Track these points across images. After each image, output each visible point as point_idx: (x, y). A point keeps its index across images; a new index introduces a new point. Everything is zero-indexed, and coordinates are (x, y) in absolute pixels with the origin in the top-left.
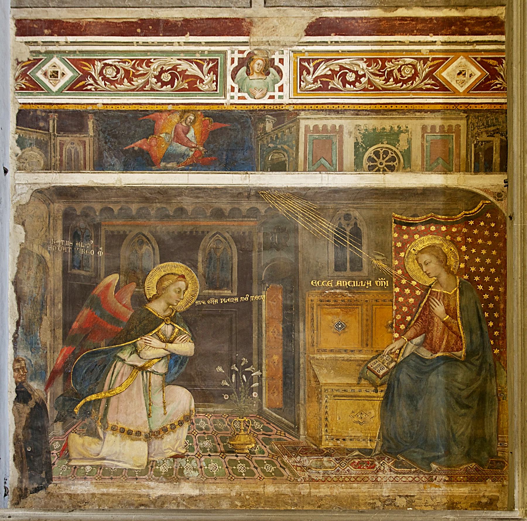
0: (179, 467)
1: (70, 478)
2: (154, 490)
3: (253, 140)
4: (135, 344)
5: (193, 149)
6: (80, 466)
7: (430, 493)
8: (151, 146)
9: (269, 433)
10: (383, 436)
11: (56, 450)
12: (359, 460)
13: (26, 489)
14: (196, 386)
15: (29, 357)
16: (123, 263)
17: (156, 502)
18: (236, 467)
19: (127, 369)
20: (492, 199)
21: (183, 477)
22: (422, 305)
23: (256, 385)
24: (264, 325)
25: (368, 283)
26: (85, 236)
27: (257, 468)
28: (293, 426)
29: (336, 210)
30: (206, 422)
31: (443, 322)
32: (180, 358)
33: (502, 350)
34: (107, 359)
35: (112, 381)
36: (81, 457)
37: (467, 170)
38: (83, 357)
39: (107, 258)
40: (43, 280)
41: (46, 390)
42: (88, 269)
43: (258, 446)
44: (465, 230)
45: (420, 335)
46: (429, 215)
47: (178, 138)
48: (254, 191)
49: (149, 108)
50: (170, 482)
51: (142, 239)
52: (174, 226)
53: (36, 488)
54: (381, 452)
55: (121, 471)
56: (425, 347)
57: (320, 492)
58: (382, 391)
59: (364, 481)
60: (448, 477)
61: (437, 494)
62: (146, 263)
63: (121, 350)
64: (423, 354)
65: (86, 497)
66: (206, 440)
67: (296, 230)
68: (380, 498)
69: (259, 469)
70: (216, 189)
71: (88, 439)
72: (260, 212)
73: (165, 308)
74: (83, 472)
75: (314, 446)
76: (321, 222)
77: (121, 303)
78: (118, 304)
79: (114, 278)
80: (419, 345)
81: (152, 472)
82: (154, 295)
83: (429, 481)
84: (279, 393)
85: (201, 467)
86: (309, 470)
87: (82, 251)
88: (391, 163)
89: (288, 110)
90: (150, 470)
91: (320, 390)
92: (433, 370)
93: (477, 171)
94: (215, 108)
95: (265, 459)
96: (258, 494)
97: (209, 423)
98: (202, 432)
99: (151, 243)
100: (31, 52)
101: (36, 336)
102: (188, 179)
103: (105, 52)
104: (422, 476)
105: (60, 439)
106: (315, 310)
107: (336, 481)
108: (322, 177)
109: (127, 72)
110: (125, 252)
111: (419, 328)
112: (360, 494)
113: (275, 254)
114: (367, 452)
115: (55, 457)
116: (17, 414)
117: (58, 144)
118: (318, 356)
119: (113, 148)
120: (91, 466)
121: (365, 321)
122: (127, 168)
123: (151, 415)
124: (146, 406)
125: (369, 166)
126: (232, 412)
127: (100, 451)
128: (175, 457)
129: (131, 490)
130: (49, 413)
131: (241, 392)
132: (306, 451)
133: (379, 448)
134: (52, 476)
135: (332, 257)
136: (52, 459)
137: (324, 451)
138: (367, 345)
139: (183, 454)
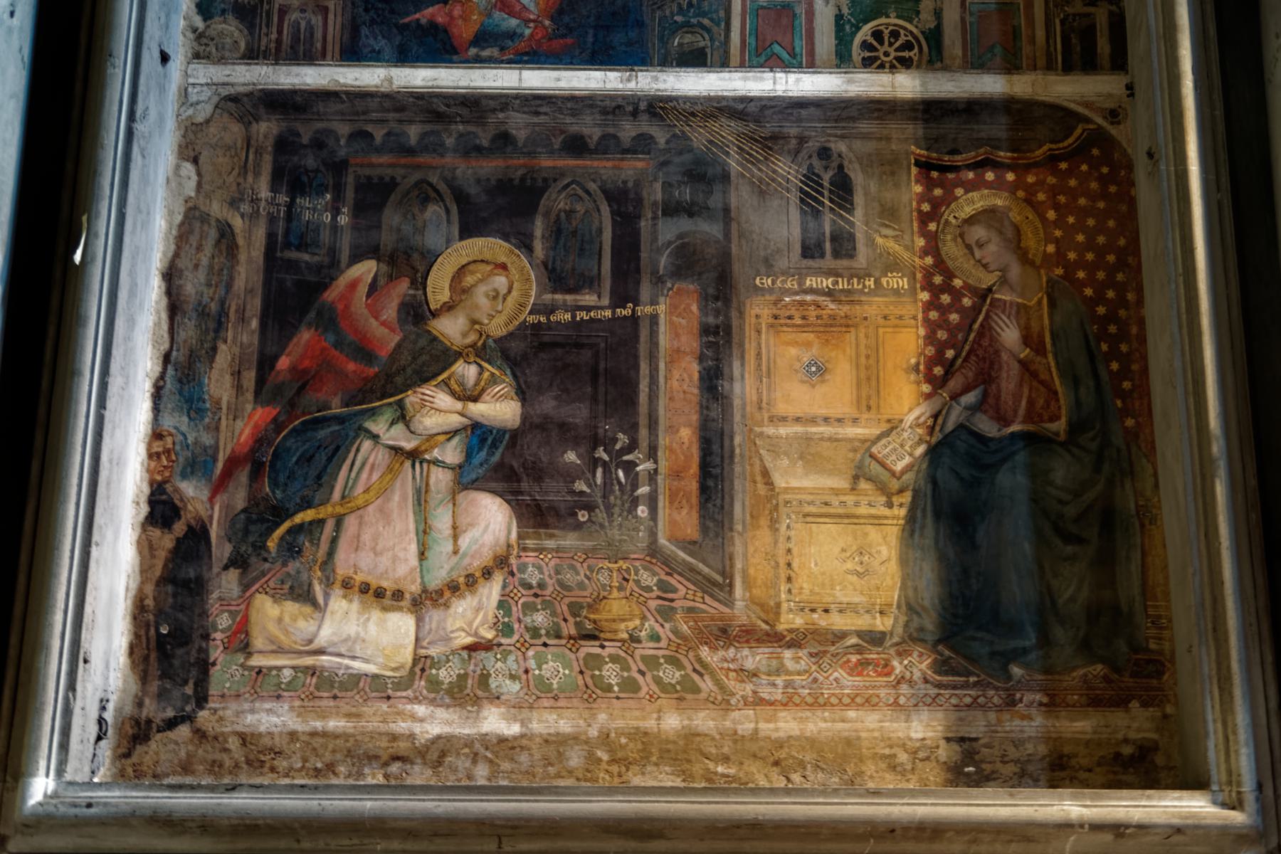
0: (479, 672)
1: (247, 695)
2: (425, 725)
3: (644, 8)
4: (400, 405)
5: (532, 25)
6: (270, 669)
7: (1012, 731)
8: (452, 18)
9: (670, 596)
10: (910, 608)
11: (223, 631)
12: (859, 657)
13: (149, 722)
14: (521, 493)
15: (184, 428)
16: (387, 239)
17: (427, 752)
18: (600, 671)
20: (1100, 121)
21: (487, 694)
22: (976, 326)
23: (643, 490)
24: (662, 366)
25: (867, 283)
26: (314, 185)
27: (642, 673)
28: (719, 579)
29: (802, 140)
31: (1020, 361)
32: (491, 432)
33: (1140, 420)
34: (343, 433)
35: (351, 482)
36: (274, 647)
37: (1050, 67)
38: (294, 430)
39: (355, 227)
40: (225, 272)
41: (211, 500)
42: (317, 251)
43: (647, 625)
44: (1051, 180)
45: (975, 387)
46: (982, 151)
48: (645, 103)
50: (460, 705)
51: (425, 194)
52: (490, 167)
53: (170, 719)
54: (903, 638)
56: (985, 412)
57: (777, 730)
58: (901, 505)
59: (870, 703)
60: (1048, 695)
61: (1025, 735)
62: (432, 239)
63: (374, 415)
64: (981, 426)
65: (277, 739)
66: (538, 610)
67: (725, 177)
68: (904, 745)
69: (649, 677)
70: (573, 98)
71: (291, 607)
72: (656, 143)
73: (466, 329)
74: (275, 681)
75: (764, 626)
76: (773, 163)
77: (376, 318)
78: (373, 321)
79: (366, 270)
80: (973, 409)
81: (423, 683)
82: (445, 303)
83: (1008, 705)
84: (691, 507)
85: (527, 672)
86: (754, 679)
87: (307, 216)
88: (906, 54)
90: (417, 677)
91: (774, 502)
92: (1004, 460)
93: (1068, 68)
95: (660, 653)
96: (646, 734)
97: (547, 573)
98: (532, 592)
99: (443, 200)
101: (200, 384)
102: (520, 80)
104: (992, 692)
106: (763, 336)
107: (811, 705)
108: (775, 78)
110: (391, 217)
111: (970, 374)
112: (863, 735)
113: (685, 224)
114: (874, 639)
115: (217, 647)
116: (146, 551)
117: (276, 11)
118: (770, 430)
119: (378, 20)
120: (293, 668)
121: (863, 360)
122: (404, 57)
123: (426, 554)
124: (417, 534)
125: (864, 59)
126: (594, 549)
127: (316, 635)
128: (471, 648)
129: (373, 725)
130: (214, 549)
131: (615, 505)
132: (749, 636)
133: (900, 630)
134: (207, 690)
135: (796, 232)
136: (211, 651)
137: (784, 637)
138: (869, 408)
139: (490, 641)
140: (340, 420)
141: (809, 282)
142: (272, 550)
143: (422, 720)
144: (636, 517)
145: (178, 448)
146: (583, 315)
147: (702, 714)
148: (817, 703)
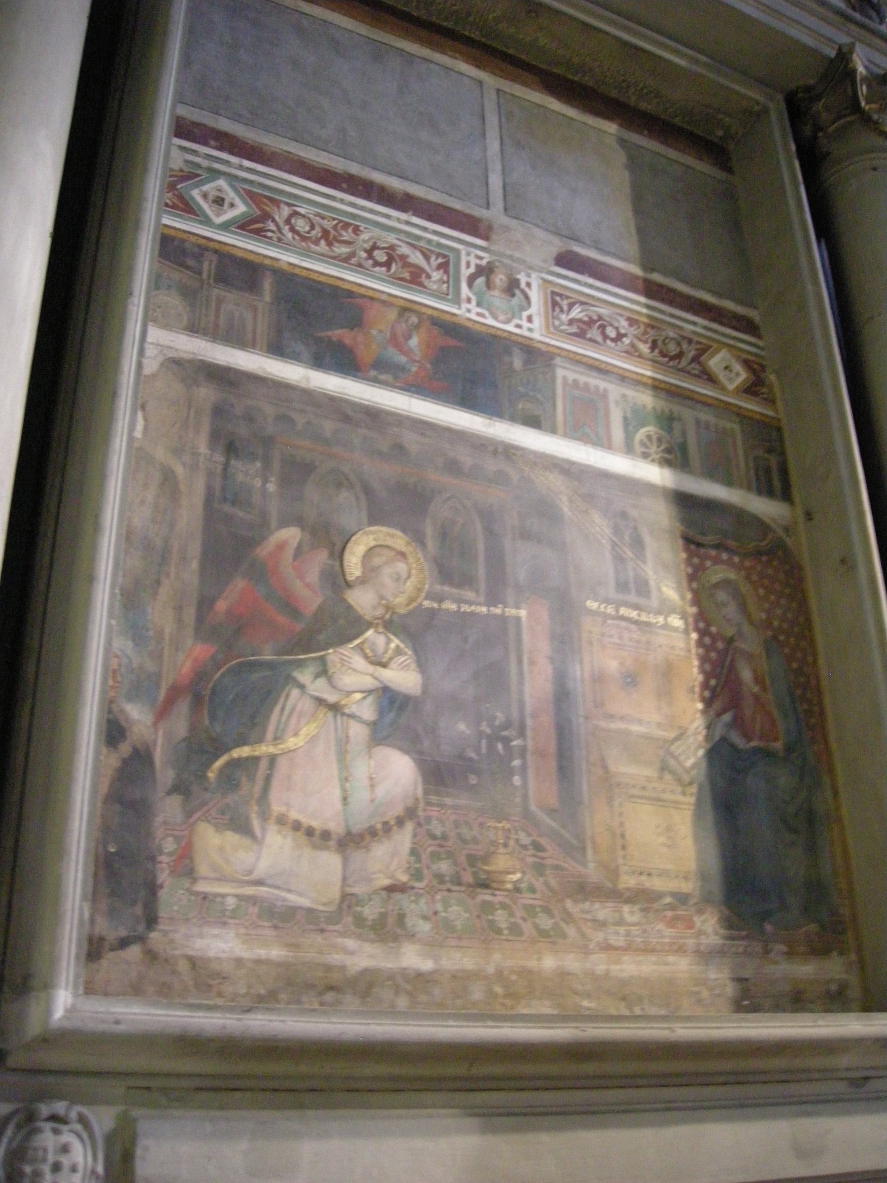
4: (322, 659)
5: (417, 364)
11: (170, 854)
13: (102, 939)
15: (129, 652)
19: (307, 705)
21: (403, 932)
22: (727, 663)
23: (516, 763)
27: (524, 919)
28: (574, 842)
30: (441, 821)
35: (282, 726)
41: (155, 724)
47: (395, 341)
49: (355, 289)
51: (340, 481)
62: (347, 520)
66: (442, 859)
71: (232, 838)
79: (291, 535)
82: (358, 578)
87: (240, 477)
89: (539, 349)
93: (760, 492)
94: (447, 317)
100: (187, 162)
103: (295, 197)
105: (179, 833)
109: (325, 233)
114: (682, 899)
122: (319, 363)
128: (391, 889)
133: (697, 893)
139: (404, 884)
140: (270, 665)
141: (623, 611)
142: (212, 780)
143: (352, 953)
144: (512, 784)
145: (123, 670)
146: (465, 608)
147: (572, 956)
148: (648, 950)
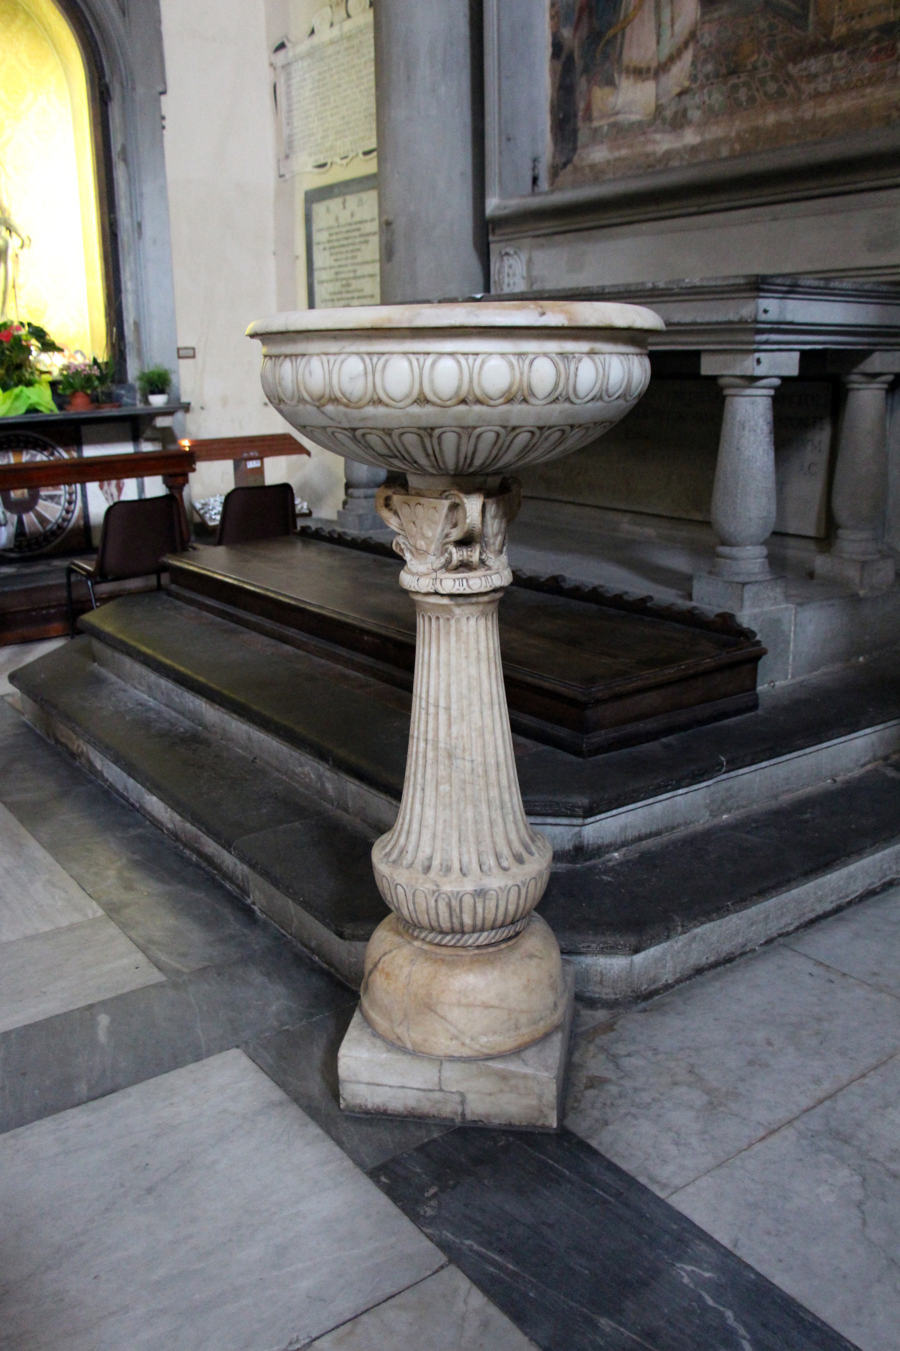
41: (574, 35)
55: (632, 125)
69: (761, 92)
71: (607, 90)
127: (616, 105)
128: (680, 94)
132: (815, 50)
139: (688, 88)
